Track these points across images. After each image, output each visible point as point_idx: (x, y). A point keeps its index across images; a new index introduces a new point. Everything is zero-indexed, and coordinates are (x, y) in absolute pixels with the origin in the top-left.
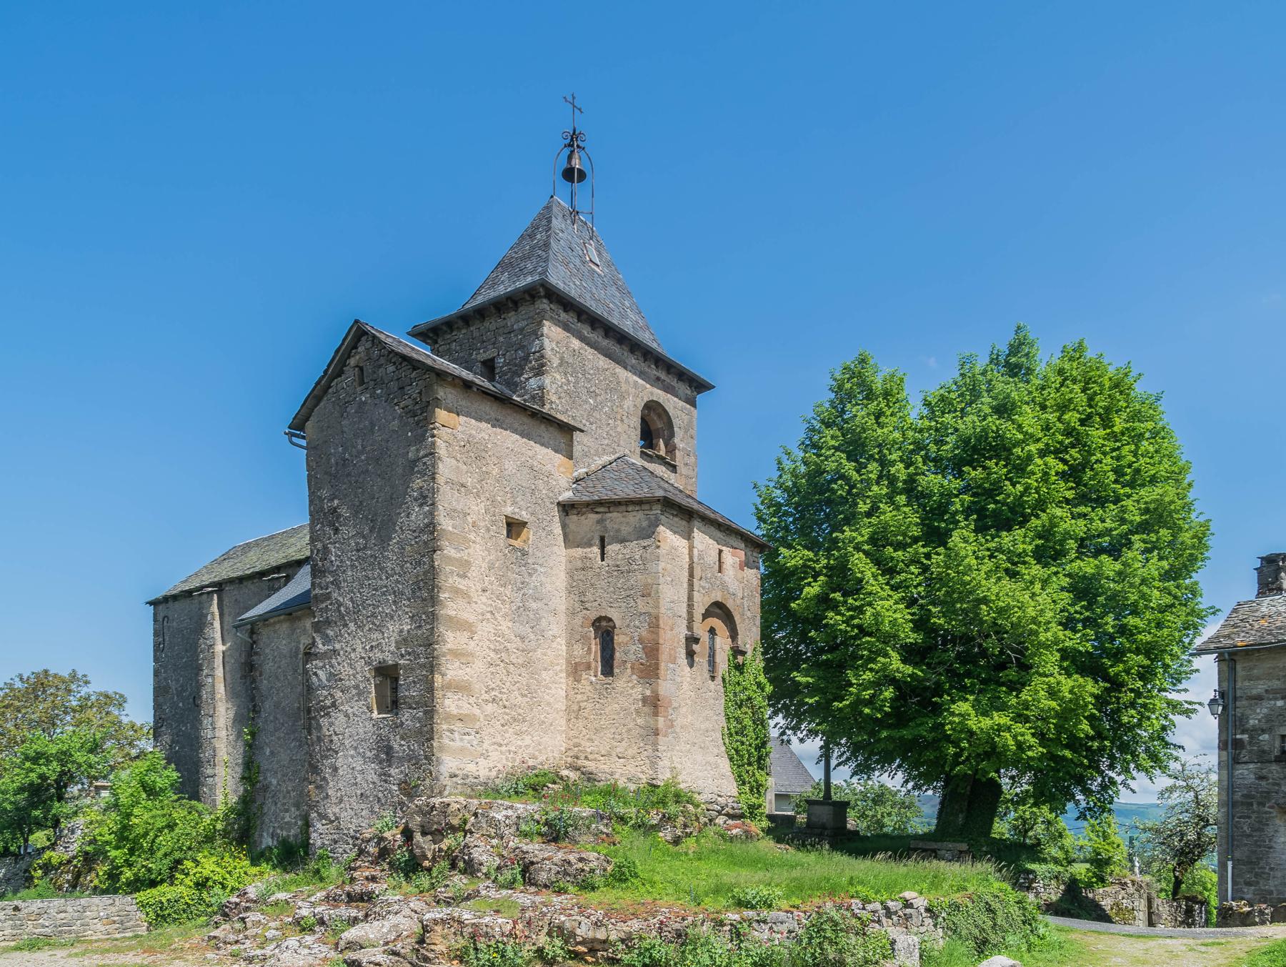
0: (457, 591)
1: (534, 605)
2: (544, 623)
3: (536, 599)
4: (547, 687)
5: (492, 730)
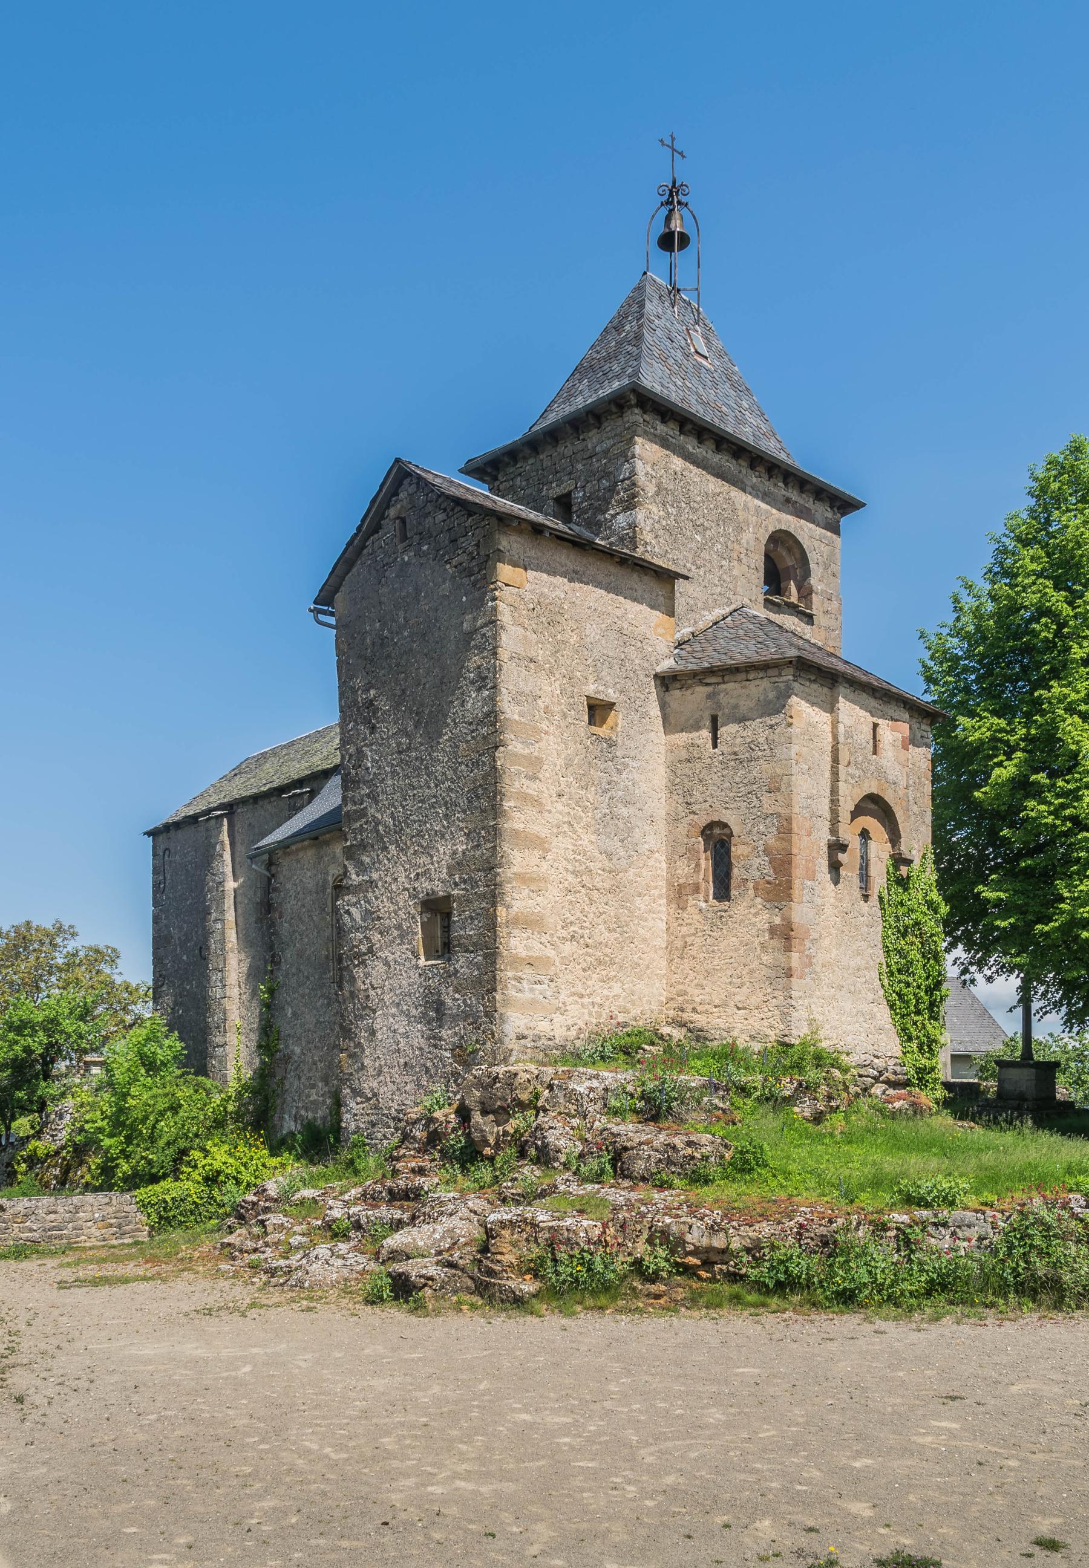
0: (525, 798)
1: (624, 811)
3: (627, 804)
4: (642, 918)
5: (571, 977)
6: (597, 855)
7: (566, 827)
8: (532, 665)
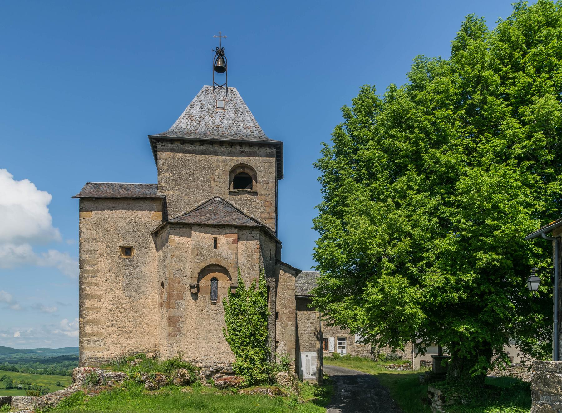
0: (91, 283)
3: (138, 279)
7: (109, 290)
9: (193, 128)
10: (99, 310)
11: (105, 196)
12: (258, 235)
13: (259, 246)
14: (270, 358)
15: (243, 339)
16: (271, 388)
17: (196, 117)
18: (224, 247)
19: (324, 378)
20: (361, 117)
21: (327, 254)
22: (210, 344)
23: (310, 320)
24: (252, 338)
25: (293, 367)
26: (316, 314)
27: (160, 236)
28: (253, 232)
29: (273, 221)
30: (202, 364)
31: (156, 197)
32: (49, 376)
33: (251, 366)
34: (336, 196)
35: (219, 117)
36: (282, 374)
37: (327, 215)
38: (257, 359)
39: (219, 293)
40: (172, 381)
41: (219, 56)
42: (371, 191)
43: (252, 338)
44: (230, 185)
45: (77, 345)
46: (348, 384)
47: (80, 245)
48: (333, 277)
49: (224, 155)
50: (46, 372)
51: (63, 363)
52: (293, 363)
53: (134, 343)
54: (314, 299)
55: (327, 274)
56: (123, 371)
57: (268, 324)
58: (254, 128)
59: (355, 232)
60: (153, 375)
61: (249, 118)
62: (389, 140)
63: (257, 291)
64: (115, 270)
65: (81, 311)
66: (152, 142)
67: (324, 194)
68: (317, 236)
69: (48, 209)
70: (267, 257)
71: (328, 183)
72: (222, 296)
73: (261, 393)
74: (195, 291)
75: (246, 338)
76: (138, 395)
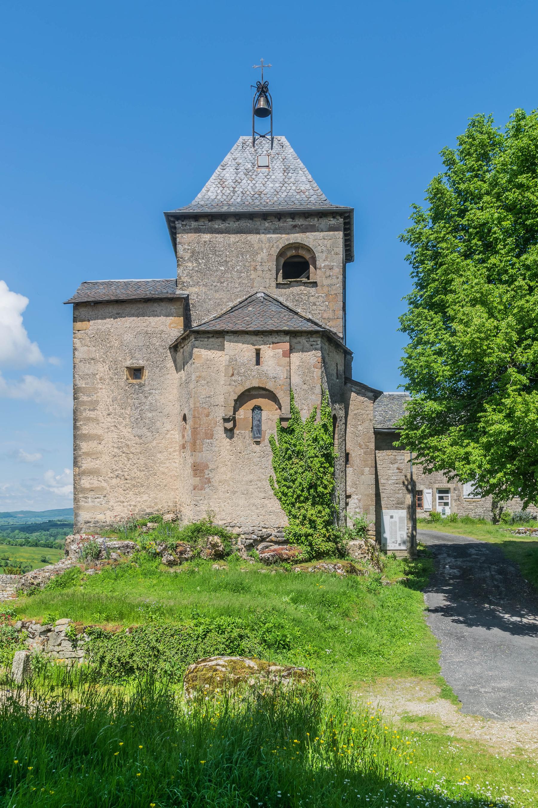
0: (89, 419)
1: (150, 415)
2: (158, 424)
3: (151, 411)
4: (161, 463)
5: (116, 494)
6: (133, 437)
7: (113, 428)
8: (92, 361)
9: (225, 197)
10: (99, 455)
11: (106, 298)
12: (319, 342)
13: (320, 359)
14: (338, 520)
15: (299, 492)
16: (341, 563)
17: (229, 182)
18: (270, 363)
19: (418, 548)
20: (471, 162)
21: (421, 366)
22: (252, 501)
23: (396, 465)
24: (312, 491)
25: (372, 532)
26: (406, 455)
27: (182, 350)
28: (312, 339)
29: (340, 322)
30: (241, 529)
31: (175, 296)
32: (32, 548)
33: (311, 531)
34: (434, 280)
35: (261, 180)
36: (357, 543)
37: (420, 309)
38: (319, 521)
39: (264, 427)
40: (199, 553)
41: (260, 94)
42: (489, 270)
43: (312, 490)
44: (277, 274)
45: (70, 505)
46: (455, 557)
47: (74, 367)
48: (431, 399)
49: (269, 233)
50: (27, 543)
51: (48, 531)
52: (372, 527)
53: (146, 501)
54: (403, 432)
55: (422, 395)
56: (132, 539)
57: (334, 471)
58: (311, 191)
59: (465, 331)
60: (172, 544)
61: (304, 178)
62: (514, 192)
63: (318, 423)
64: (121, 399)
65: (75, 458)
66: (169, 222)
67: (416, 279)
68: (406, 340)
69: (21, 319)
70: (332, 375)
71: (422, 262)
72: (268, 431)
73: (326, 571)
74: (230, 425)
75: (302, 491)
76: (153, 573)
